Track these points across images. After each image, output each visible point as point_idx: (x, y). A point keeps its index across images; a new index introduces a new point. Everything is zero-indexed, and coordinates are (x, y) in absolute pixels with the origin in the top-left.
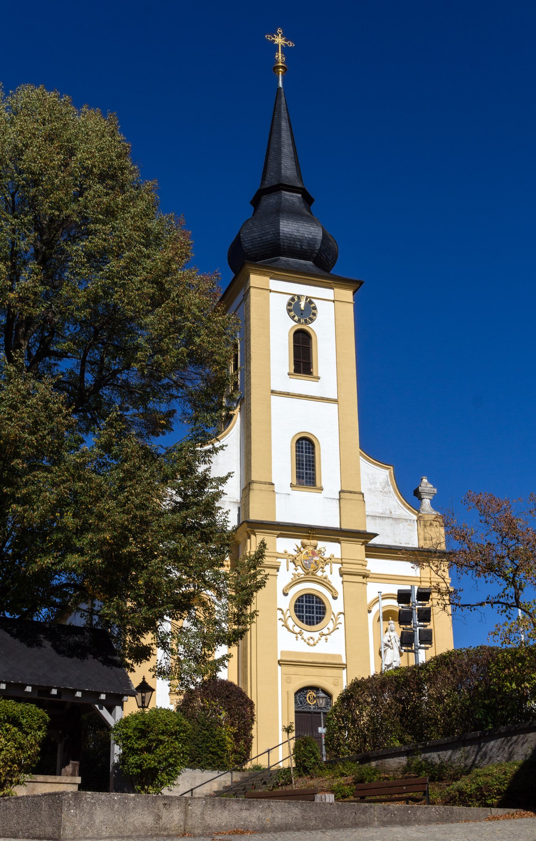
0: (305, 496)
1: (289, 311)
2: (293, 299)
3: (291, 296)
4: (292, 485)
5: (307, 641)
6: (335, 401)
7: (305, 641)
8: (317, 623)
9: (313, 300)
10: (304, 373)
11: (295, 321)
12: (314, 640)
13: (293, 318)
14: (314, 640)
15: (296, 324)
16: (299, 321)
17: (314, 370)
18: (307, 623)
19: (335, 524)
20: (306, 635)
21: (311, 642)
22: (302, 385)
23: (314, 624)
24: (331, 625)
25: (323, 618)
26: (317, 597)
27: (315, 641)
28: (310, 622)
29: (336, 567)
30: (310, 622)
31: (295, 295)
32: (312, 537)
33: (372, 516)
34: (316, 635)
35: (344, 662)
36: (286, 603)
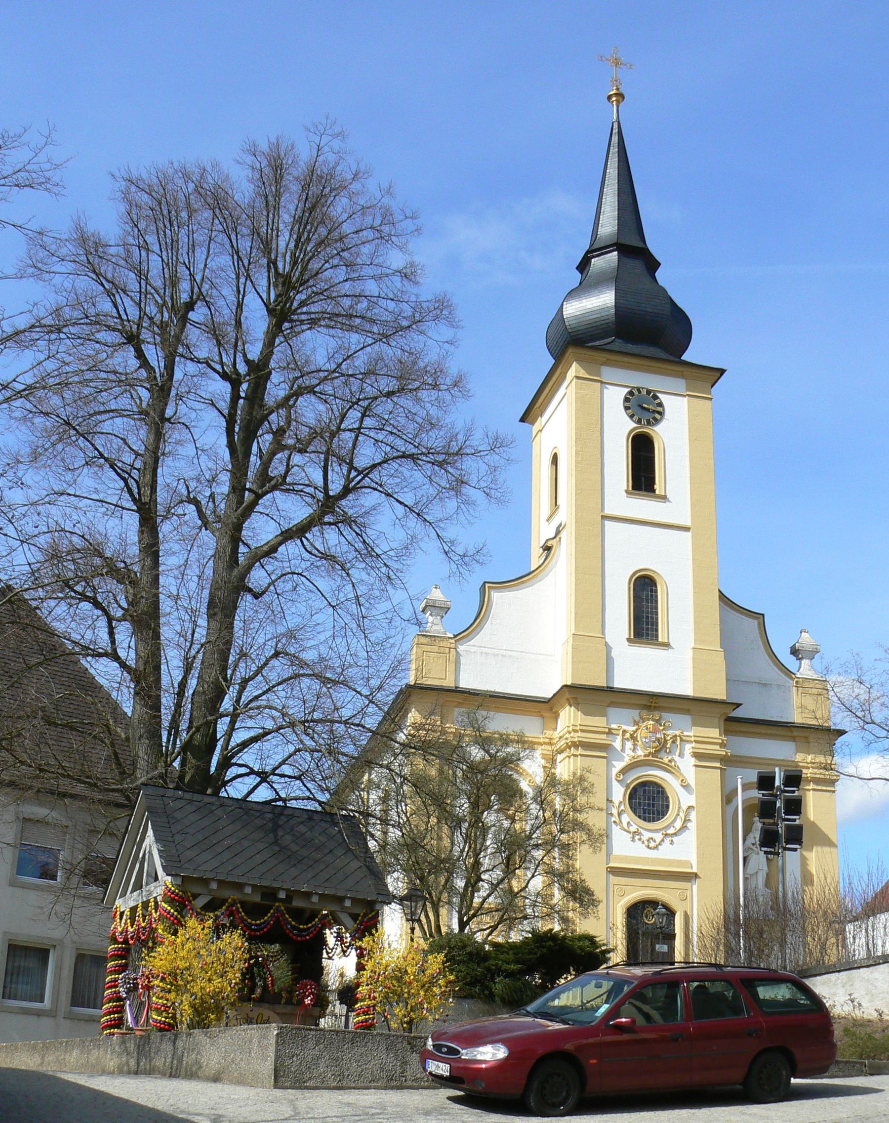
1: (627, 408)
2: (631, 393)
3: (628, 390)
5: (646, 842)
6: (686, 529)
7: (643, 843)
9: (659, 395)
10: (646, 490)
11: (634, 421)
12: (655, 841)
13: (631, 417)
14: (655, 841)
15: (636, 425)
16: (639, 422)
17: (658, 488)
19: (689, 692)
20: (646, 835)
21: (652, 844)
22: (642, 507)
24: (678, 824)
29: (688, 748)
32: (655, 707)
34: (658, 837)
35: (695, 870)
36: (619, 793)
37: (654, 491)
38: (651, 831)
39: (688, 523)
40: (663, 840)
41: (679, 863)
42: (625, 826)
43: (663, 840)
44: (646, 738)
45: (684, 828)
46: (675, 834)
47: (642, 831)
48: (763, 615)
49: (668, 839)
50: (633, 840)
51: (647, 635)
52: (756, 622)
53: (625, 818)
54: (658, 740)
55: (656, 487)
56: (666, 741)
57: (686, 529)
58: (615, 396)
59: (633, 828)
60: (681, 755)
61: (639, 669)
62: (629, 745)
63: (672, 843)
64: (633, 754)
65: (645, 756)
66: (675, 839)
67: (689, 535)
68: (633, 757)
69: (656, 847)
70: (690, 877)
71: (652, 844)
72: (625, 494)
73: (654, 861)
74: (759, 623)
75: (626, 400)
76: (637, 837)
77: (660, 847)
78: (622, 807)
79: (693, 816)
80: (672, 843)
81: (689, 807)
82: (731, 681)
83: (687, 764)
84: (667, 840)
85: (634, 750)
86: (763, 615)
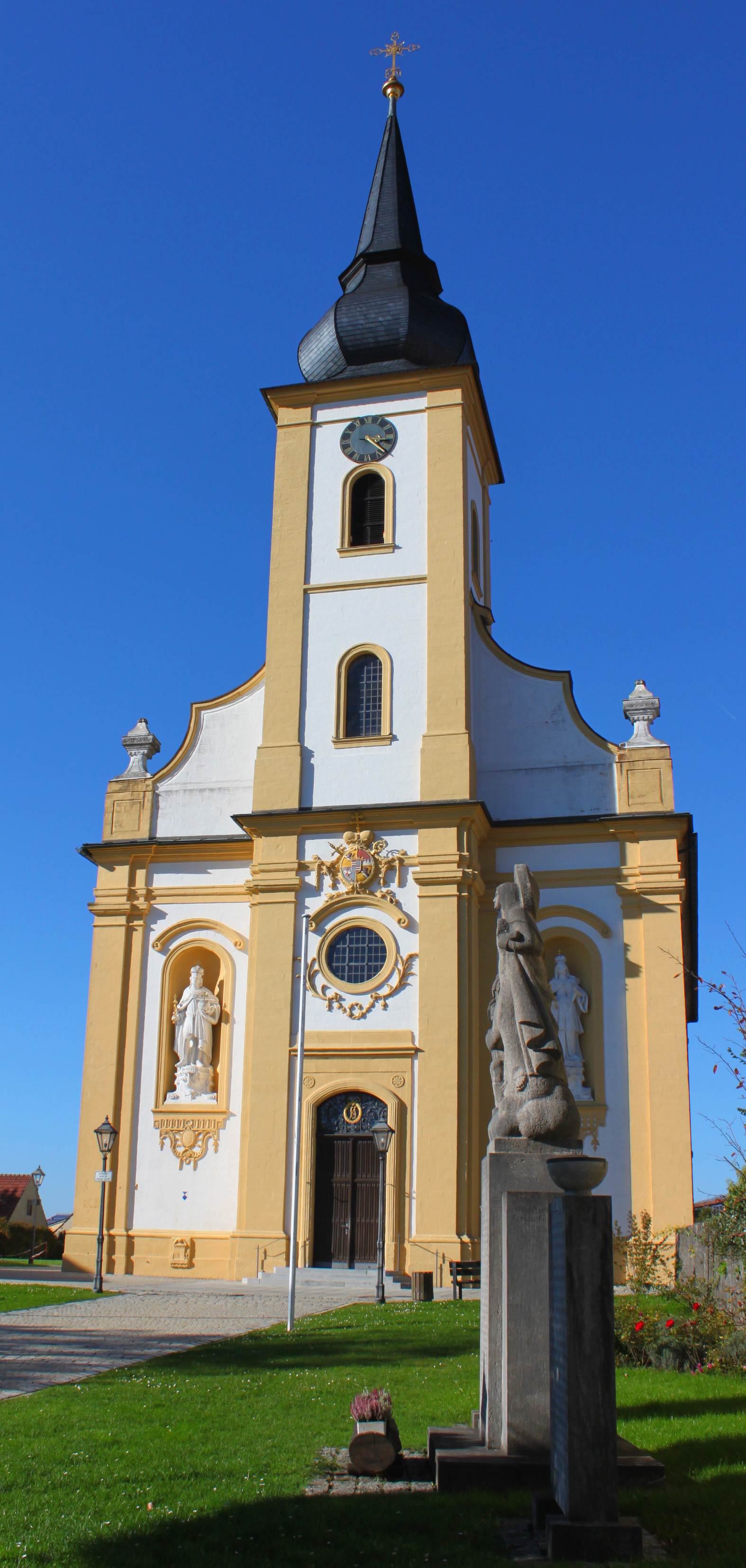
0: (363, 753)
1: (344, 447)
2: (351, 428)
3: (348, 423)
4: (337, 741)
5: (348, 1010)
6: (420, 579)
8: (369, 977)
9: (389, 419)
10: (372, 543)
11: (355, 461)
14: (361, 1008)
17: (387, 536)
18: (349, 981)
19: (414, 795)
22: (369, 564)
23: (362, 980)
24: (395, 981)
25: (382, 966)
26: (371, 931)
27: (364, 1011)
28: (355, 976)
30: (356, 976)
31: (355, 419)
33: (526, 770)
35: (417, 1044)
37: (382, 541)
38: (354, 995)
39: (424, 572)
40: (373, 1006)
41: (395, 1035)
42: (319, 990)
43: (373, 1006)
44: (348, 869)
45: (403, 984)
46: (390, 995)
47: (344, 995)
48: (569, 672)
49: (381, 1002)
50: (330, 1008)
51: (367, 730)
52: (560, 683)
53: (320, 981)
54: (366, 870)
55: (385, 535)
56: (377, 870)
57: (420, 579)
58: (329, 439)
59: (330, 993)
60: (402, 884)
61: (349, 776)
62: (328, 880)
63: (385, 1006)
64: (334, 893)
65: (347, 893)
66: (389, 1001)
67: (424, 587)
68: (332, 898)
69: (363, 1016)
70: (414, 1053)
71: (357, 1012)
72: (338, 554)
73: (357, 1036)
74: (564, 685)
75: (345, 436)
76: (335, 1005)
77: (368, 1015)
78: (316, 967)
79: (416, 967)
80: (385, 1006)
81: (412, 957)
82: (478, 772)
83: (410, 895)
84: (379, 1004)
85: (334, 887)
86: (569, 672)
